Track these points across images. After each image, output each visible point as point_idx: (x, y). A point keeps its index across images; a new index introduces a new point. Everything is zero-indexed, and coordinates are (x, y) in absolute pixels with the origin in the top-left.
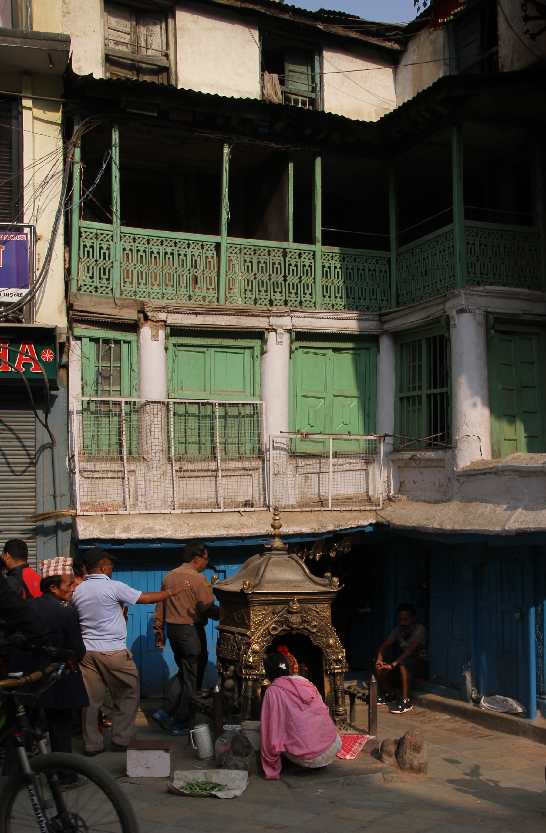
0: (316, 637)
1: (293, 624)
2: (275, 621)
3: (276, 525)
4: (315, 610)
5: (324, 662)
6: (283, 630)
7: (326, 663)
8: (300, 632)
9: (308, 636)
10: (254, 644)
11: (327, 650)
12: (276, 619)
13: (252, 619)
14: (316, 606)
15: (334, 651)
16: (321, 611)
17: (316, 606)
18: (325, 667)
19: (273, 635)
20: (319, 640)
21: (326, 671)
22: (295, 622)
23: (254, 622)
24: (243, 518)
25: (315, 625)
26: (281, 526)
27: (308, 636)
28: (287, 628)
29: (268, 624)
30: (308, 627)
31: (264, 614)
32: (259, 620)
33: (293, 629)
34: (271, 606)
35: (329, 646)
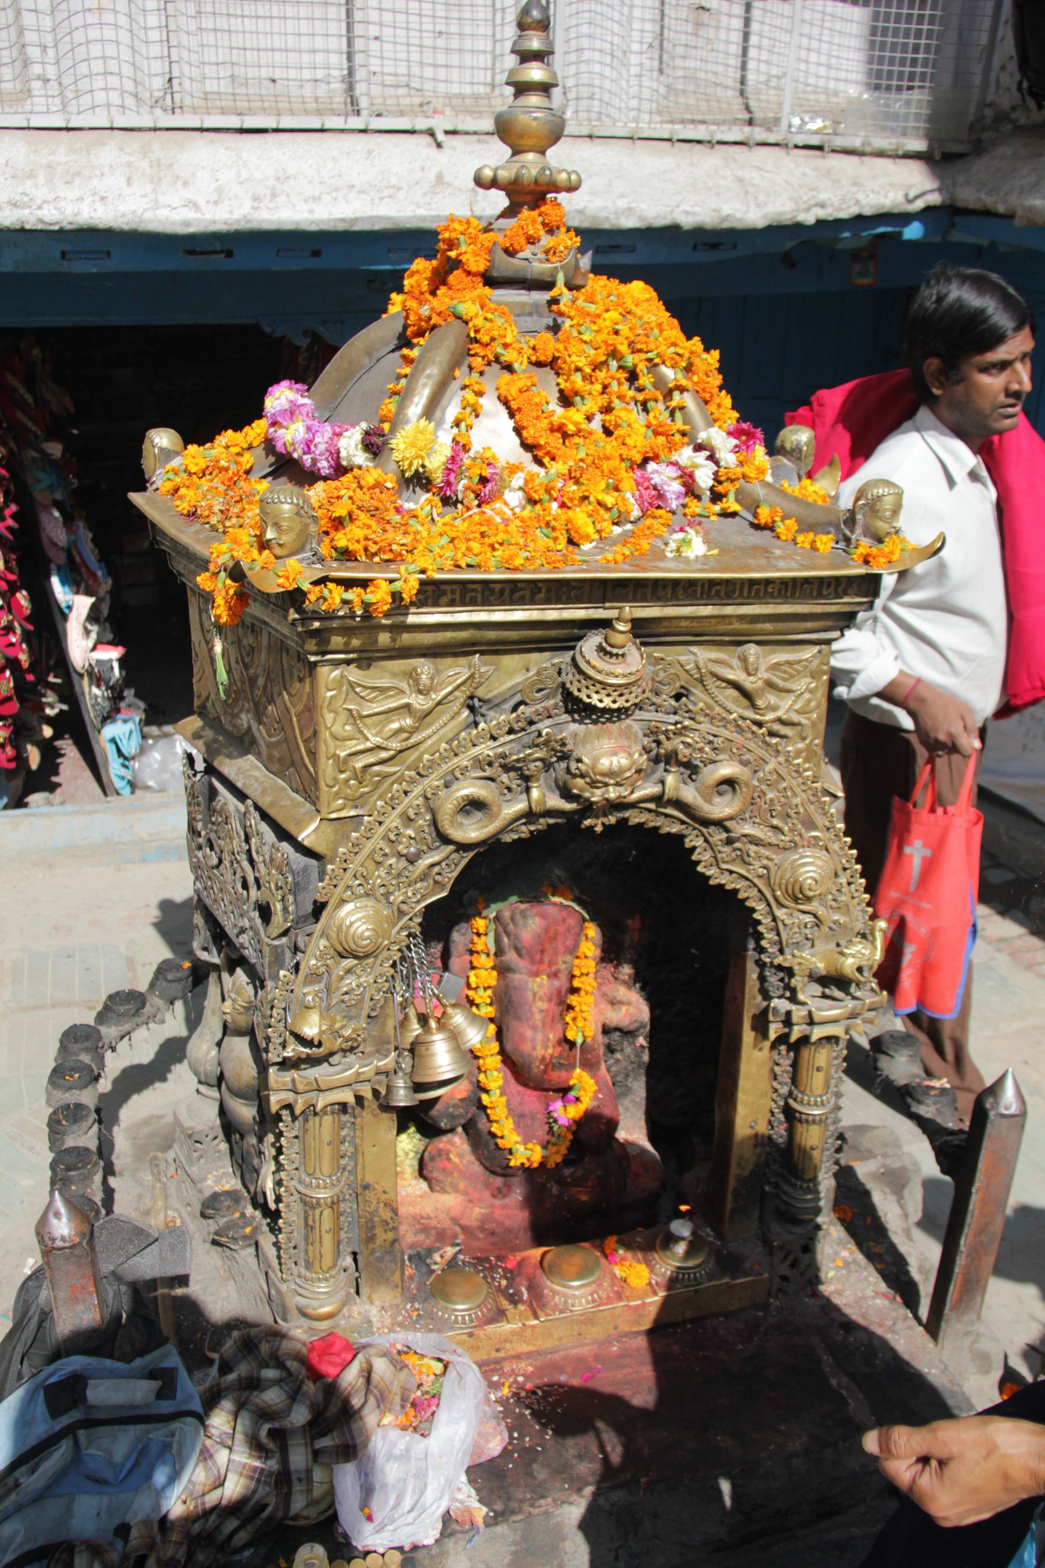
0: (729, 842)
1: (593, 784)
2: (479, 763)
3: (524, 119)
4: (736, 686)
5: (752, 974)
6: (529, 816)
7: (762, 979)
8: (635, 818)
9: (680, 838)
10: (343, 901)
11: (780, 913)
12: (486, 749)
13: (326, 746)
14: (744, 660)
15: (818, 922)
16: (770, 685)
17: (744, 660)
18: (753, 1003)
19: (462, 847)
20: (743, 859)
21: (761, 1024)
22: (611, 774)
23: (341, 765)
24: (446, 152)
25: (730, 782)
26: (555, 134)
27: (680, 838)
28: (555, 802)
29: (434, 781)
30: (689, 794)
31: (407, 707)
32: (379, 748)
33: (588, 808)
34: (462, 660)
35: (798, 896)
